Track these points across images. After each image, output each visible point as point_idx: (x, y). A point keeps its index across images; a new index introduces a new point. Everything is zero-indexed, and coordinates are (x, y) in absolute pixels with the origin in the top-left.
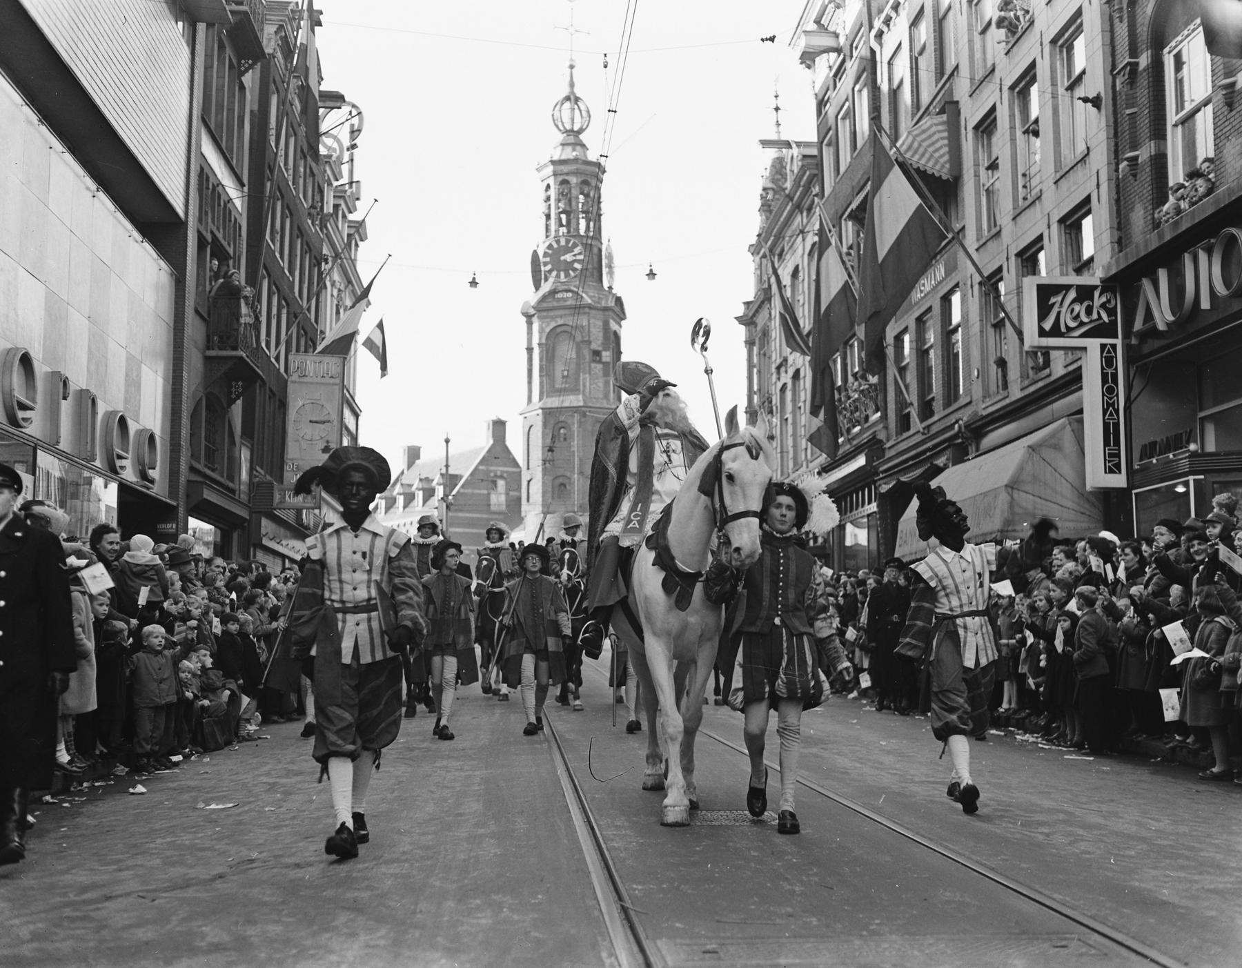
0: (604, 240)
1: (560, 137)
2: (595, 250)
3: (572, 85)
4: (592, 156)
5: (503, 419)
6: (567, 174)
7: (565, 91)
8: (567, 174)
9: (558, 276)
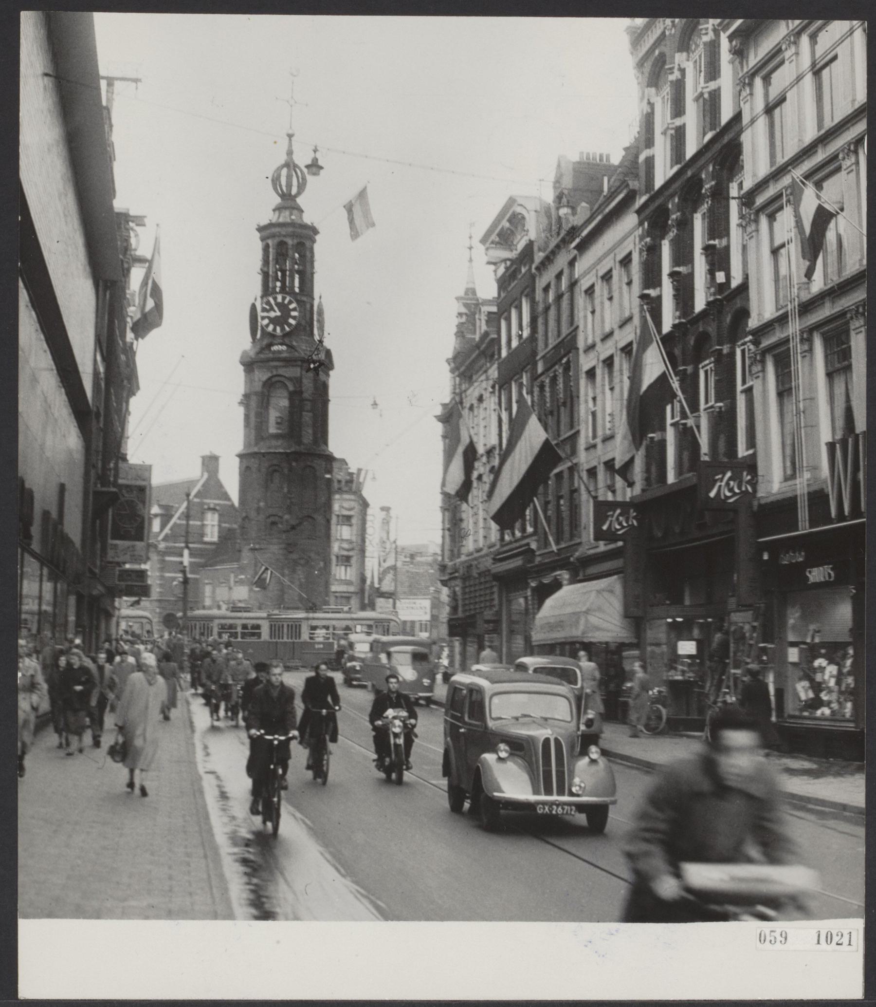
0: (316, 296)
1: (278, 200)
2: (308, 306)
3: (290, 153)
4: (307, 219)
5: (217, 453)
6: (285, 236)
7: (282, 159)
8: (285, 236)
9: (274, 330)
